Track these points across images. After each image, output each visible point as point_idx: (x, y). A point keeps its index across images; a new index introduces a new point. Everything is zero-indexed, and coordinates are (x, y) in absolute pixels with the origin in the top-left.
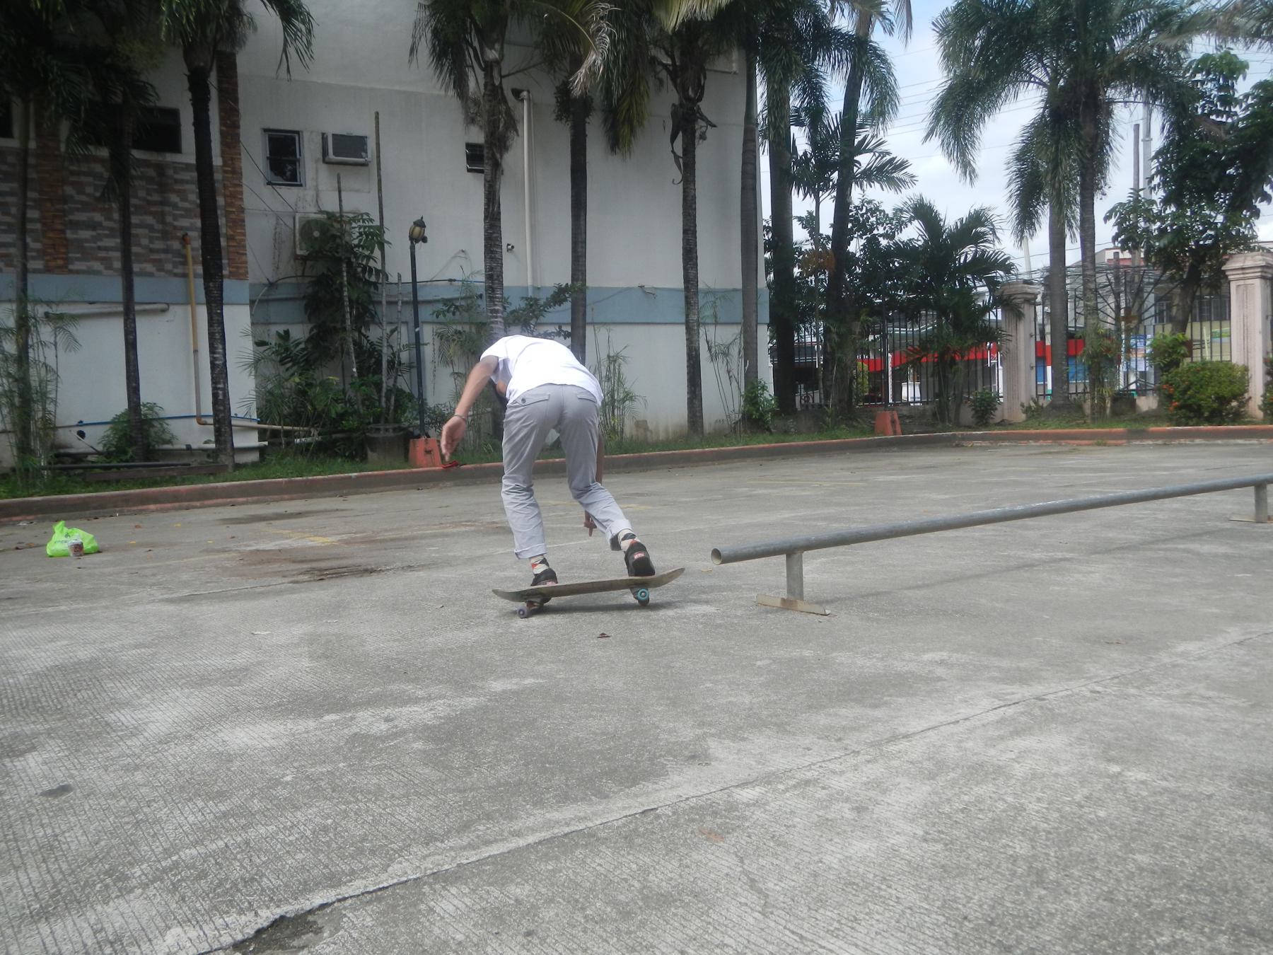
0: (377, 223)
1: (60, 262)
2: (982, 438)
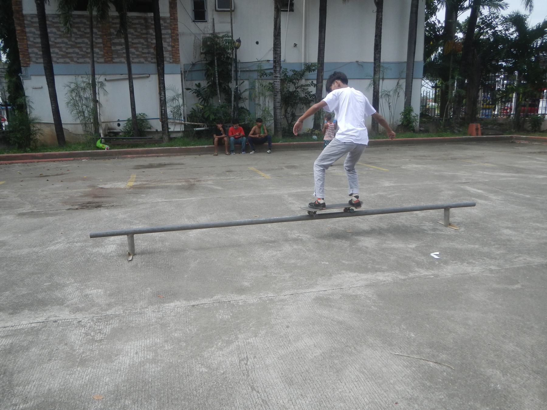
0: (230, 38)
1: (110, 59)
2: (525, 139)
